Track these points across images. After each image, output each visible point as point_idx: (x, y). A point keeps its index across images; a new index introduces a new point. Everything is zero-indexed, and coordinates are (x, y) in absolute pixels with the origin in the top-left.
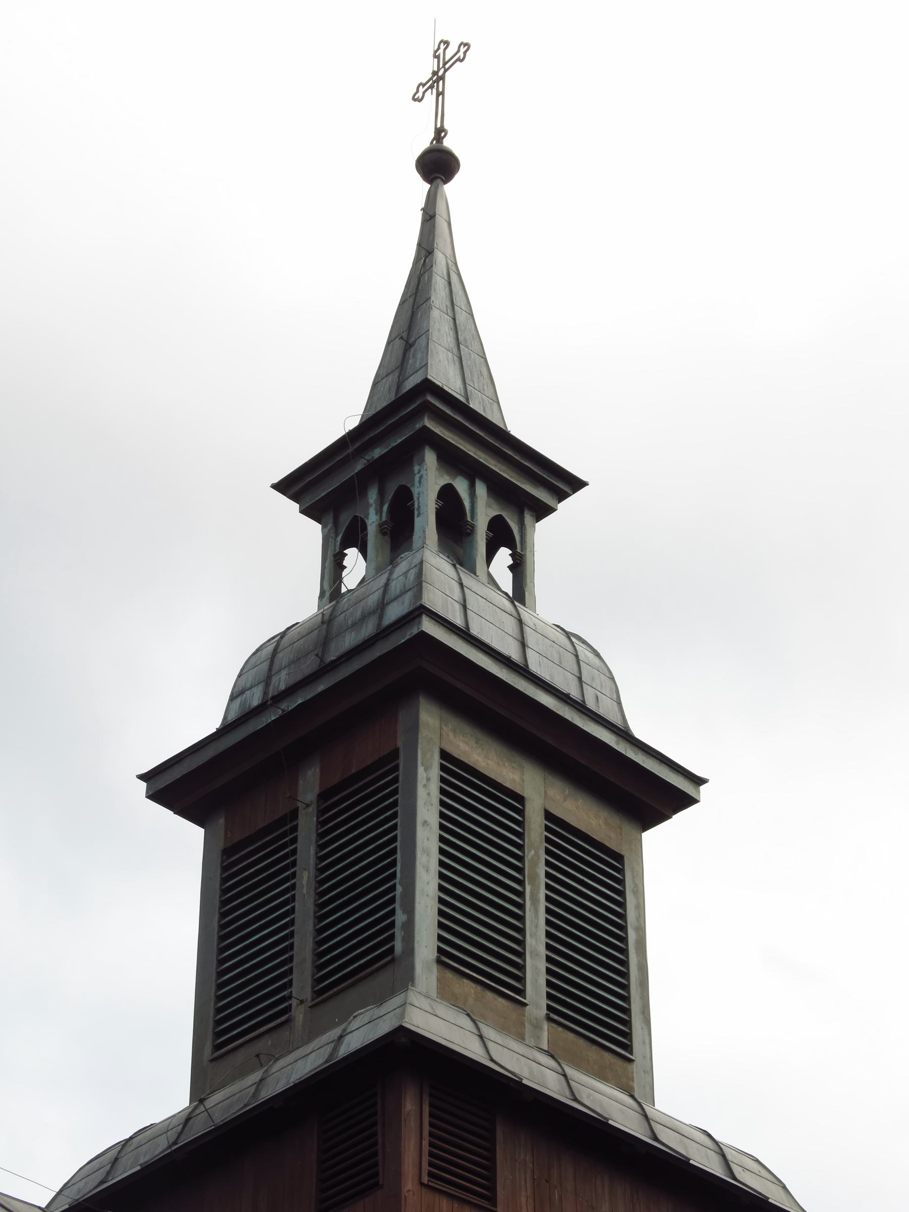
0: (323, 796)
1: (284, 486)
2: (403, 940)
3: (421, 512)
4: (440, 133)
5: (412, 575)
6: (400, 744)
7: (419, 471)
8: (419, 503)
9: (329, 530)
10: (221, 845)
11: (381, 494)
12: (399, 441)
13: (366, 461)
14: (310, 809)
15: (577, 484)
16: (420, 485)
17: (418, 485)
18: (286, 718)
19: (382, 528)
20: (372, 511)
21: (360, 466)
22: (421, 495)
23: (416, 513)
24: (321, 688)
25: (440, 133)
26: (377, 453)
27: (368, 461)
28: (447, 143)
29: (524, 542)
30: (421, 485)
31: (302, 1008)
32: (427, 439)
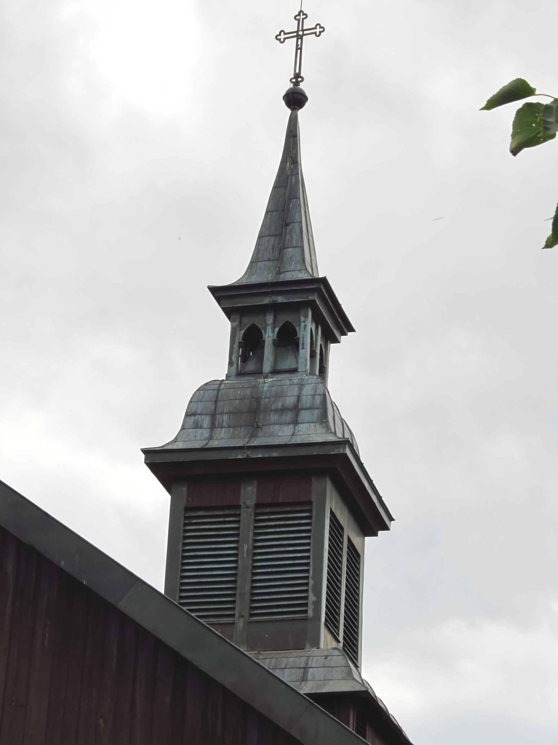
0: (257, 506)
1: (215, 291)
2: (314, 610)
3: (304, 347)
4: (297, 77)
5: (318, 399)
6: (314, 499)
7: (304, 322)
8: (303, 341)
9: (237, 326)
10: (183, 504)
11: (275, 320)
12: (296, 300)
13: (272, 301)
14: (250, 510)
15: (352, 330)
16: (304, 330)
17: (303, 329)
18: (248, 461)
19: (274, 342)
20: (269, 329)
21: (266, 301)
22: (305, 337)
23: (301, 346)
24: (275, 454)
25: (297, 77)
26: (280, 299)
27: (273, 301)
28: (302, 86)
29: (327, 360)
30: (305, 330)
31: (242, 620)
32: (312, 305)
